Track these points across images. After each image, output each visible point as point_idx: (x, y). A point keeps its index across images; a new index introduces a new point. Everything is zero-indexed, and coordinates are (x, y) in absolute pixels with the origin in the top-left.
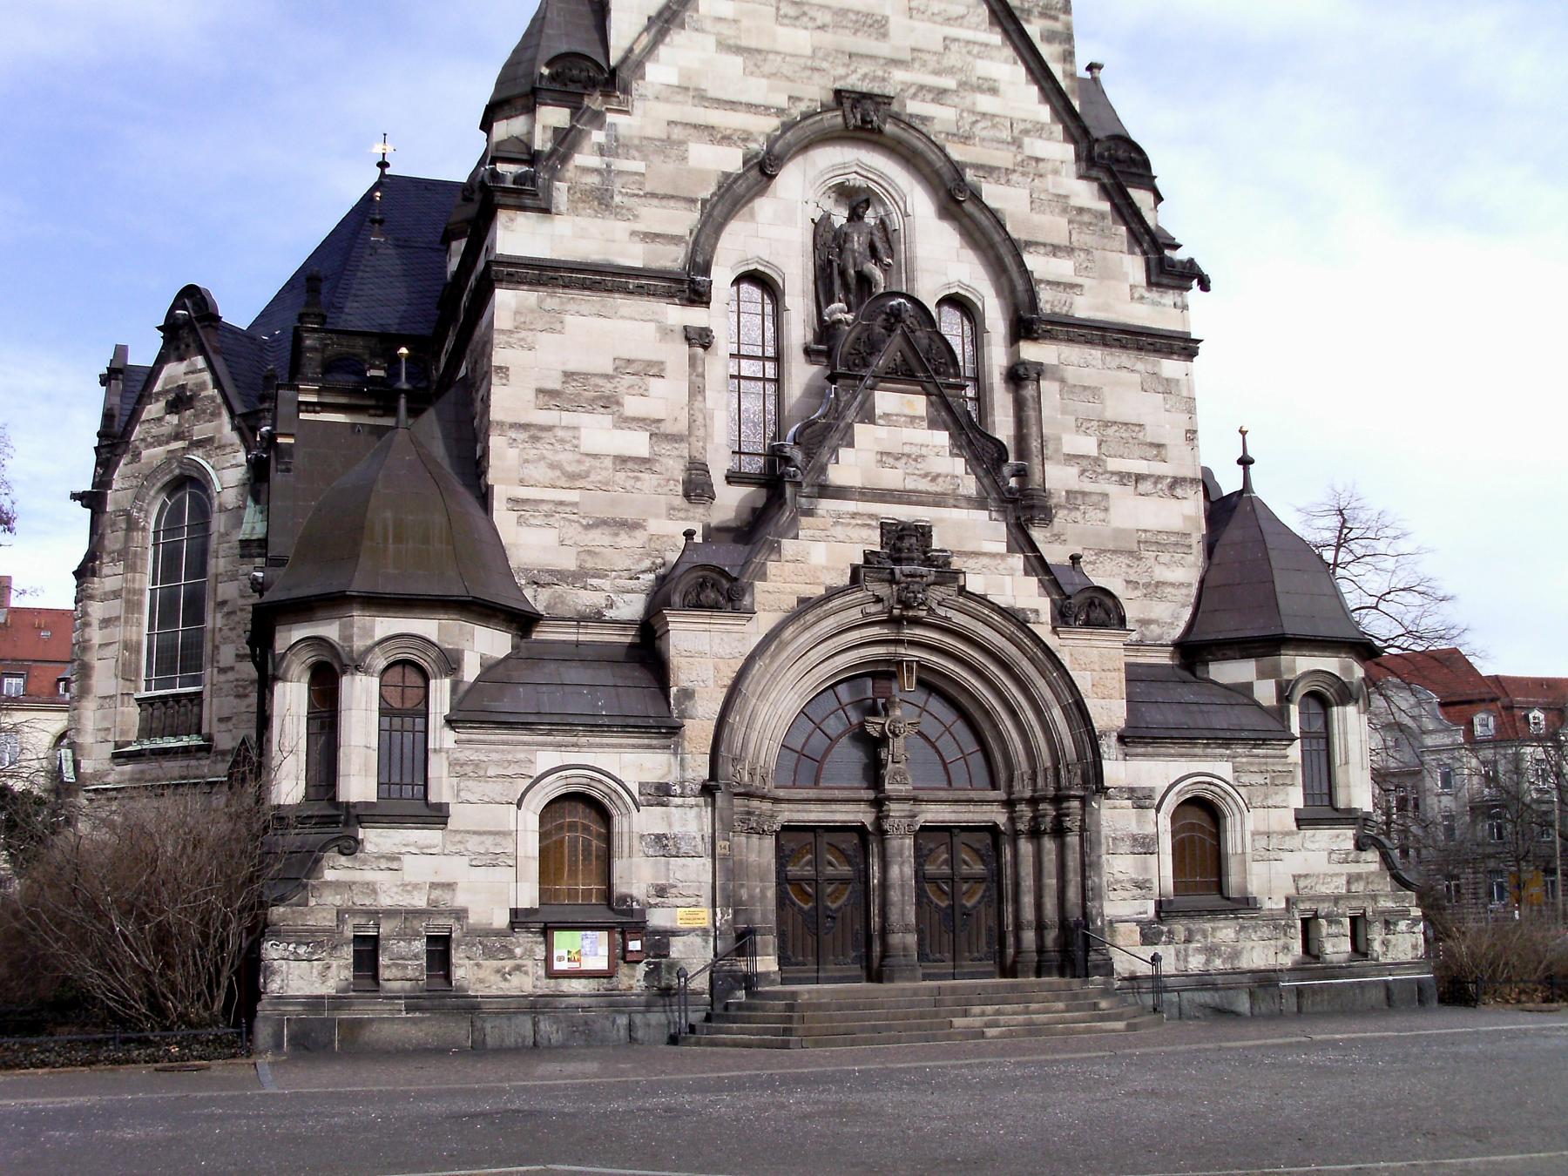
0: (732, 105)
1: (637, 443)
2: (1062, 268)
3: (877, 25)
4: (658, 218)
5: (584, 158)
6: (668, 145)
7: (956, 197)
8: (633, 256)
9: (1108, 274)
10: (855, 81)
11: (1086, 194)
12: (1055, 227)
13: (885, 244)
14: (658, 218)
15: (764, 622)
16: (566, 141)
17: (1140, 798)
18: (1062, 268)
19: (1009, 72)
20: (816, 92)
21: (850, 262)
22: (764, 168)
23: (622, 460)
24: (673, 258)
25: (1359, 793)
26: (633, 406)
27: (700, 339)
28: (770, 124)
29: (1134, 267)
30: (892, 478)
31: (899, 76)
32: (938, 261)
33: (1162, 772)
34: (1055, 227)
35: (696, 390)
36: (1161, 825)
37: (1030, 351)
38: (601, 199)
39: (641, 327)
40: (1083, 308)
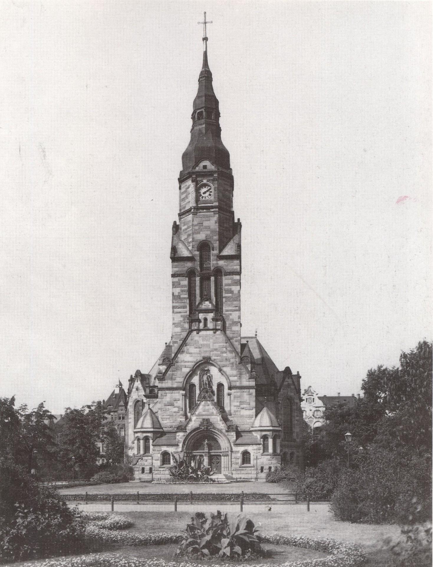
0: (188, 362)
1: (176, 409)
5: (169, 372)
8: (175, 386)
15: (188, 431)
17: (237, 452)
20: (199, 358)
23: (175, 412)
24: (180, 385)
25: (271, 450)
26: (176, 404)
28: (194, 364)
30: (204, 413)
31: (212, 353)
33: (242, 449)
36: (239, 455)
37: (230, 391)
40: (238, 384)
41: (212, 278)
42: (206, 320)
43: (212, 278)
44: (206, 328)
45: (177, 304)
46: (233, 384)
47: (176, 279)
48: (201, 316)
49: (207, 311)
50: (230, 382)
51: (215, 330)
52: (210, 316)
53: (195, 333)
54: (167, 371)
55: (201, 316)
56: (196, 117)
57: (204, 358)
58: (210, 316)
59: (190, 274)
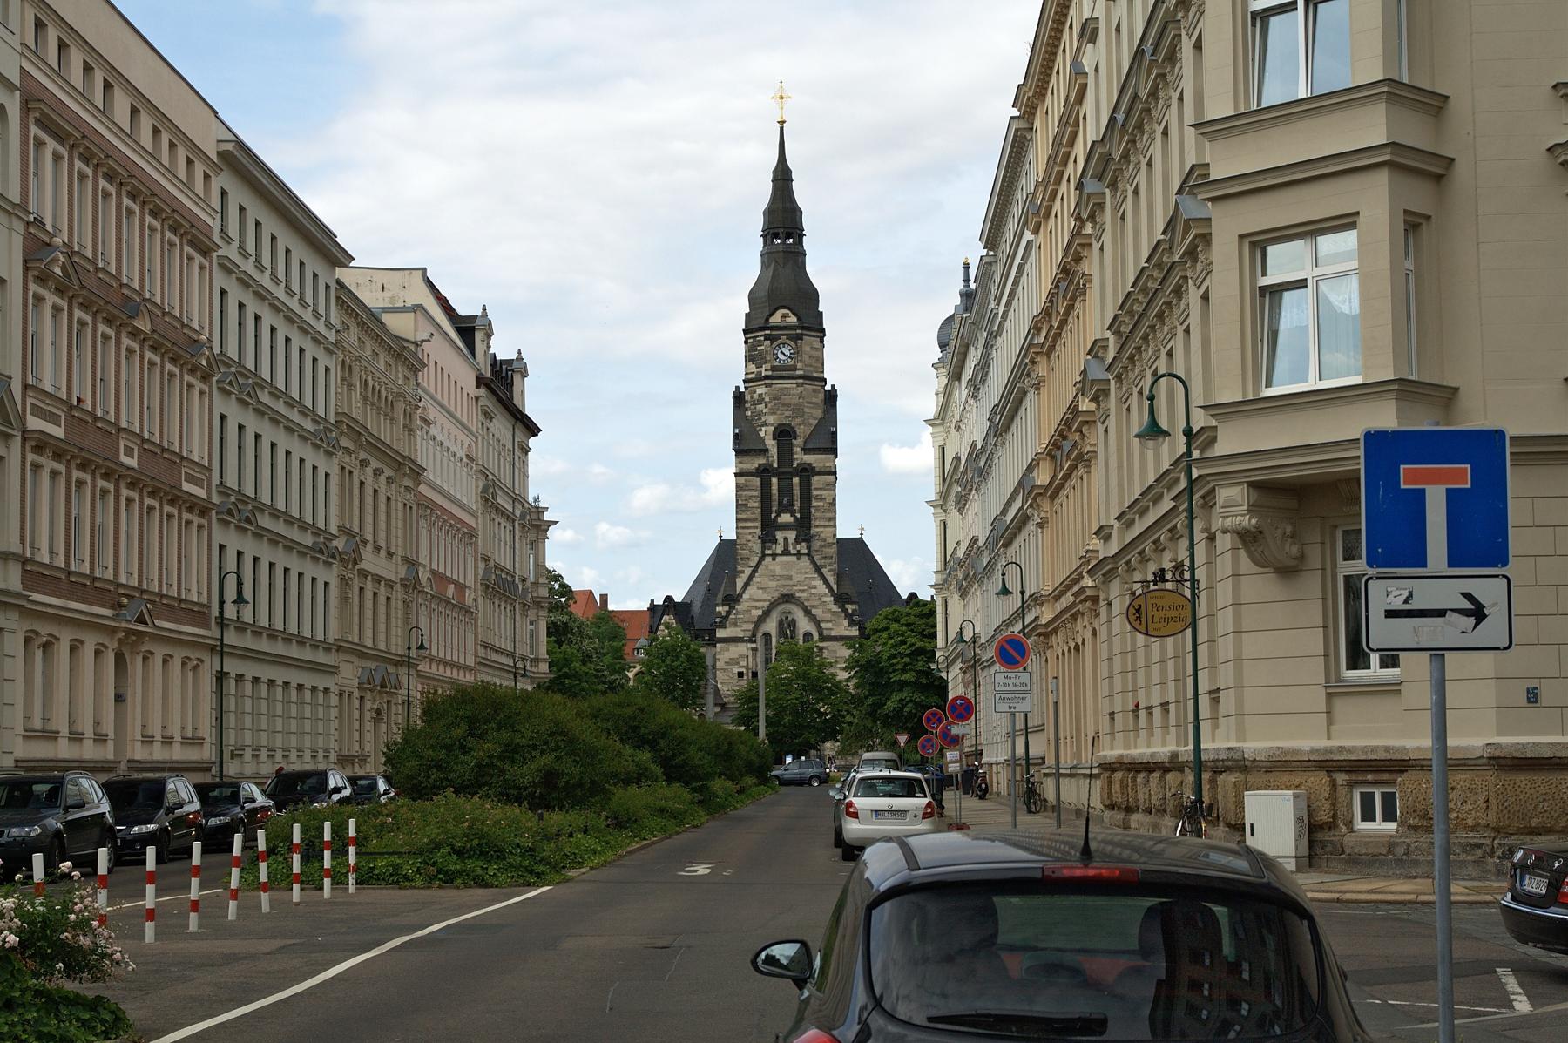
2: (830, 625)
3: (790, 578)
4: (746, 626)
6: (748, 611)
7: (807, 612)
9: (839, 625)
10: (785, 591)
11: (835, 608)
12: (828, 616)
13: (794, 621)
14: (746, 626)
16: (728, 613)
18: (830, 625)
19: (819, 583)
20: (776, 595)
21: (786, 627)
22: (767, 613)
27: (755, 650)
29: (846, 623)
32: (804, 625)
34: (828, 616)
35: (755, 659)
38: (735, 625)
39: (741, 649)
41: (796, 480)
42: (786, 539)
43: (796, 480)
44: (786, 553)
45: (743, 516)
46: (825, 633)
47: (742, 480)
48: (780, 535)
49: (785, 527)
50: (821, 634)
51: (799, 555)
52: (792, 535)
53: (768, 559)
54: (728, 613)
55: (780, 535)
56: (769, 234)
57: (783, 596)
58: (792, 535)
59: (764, 472)
